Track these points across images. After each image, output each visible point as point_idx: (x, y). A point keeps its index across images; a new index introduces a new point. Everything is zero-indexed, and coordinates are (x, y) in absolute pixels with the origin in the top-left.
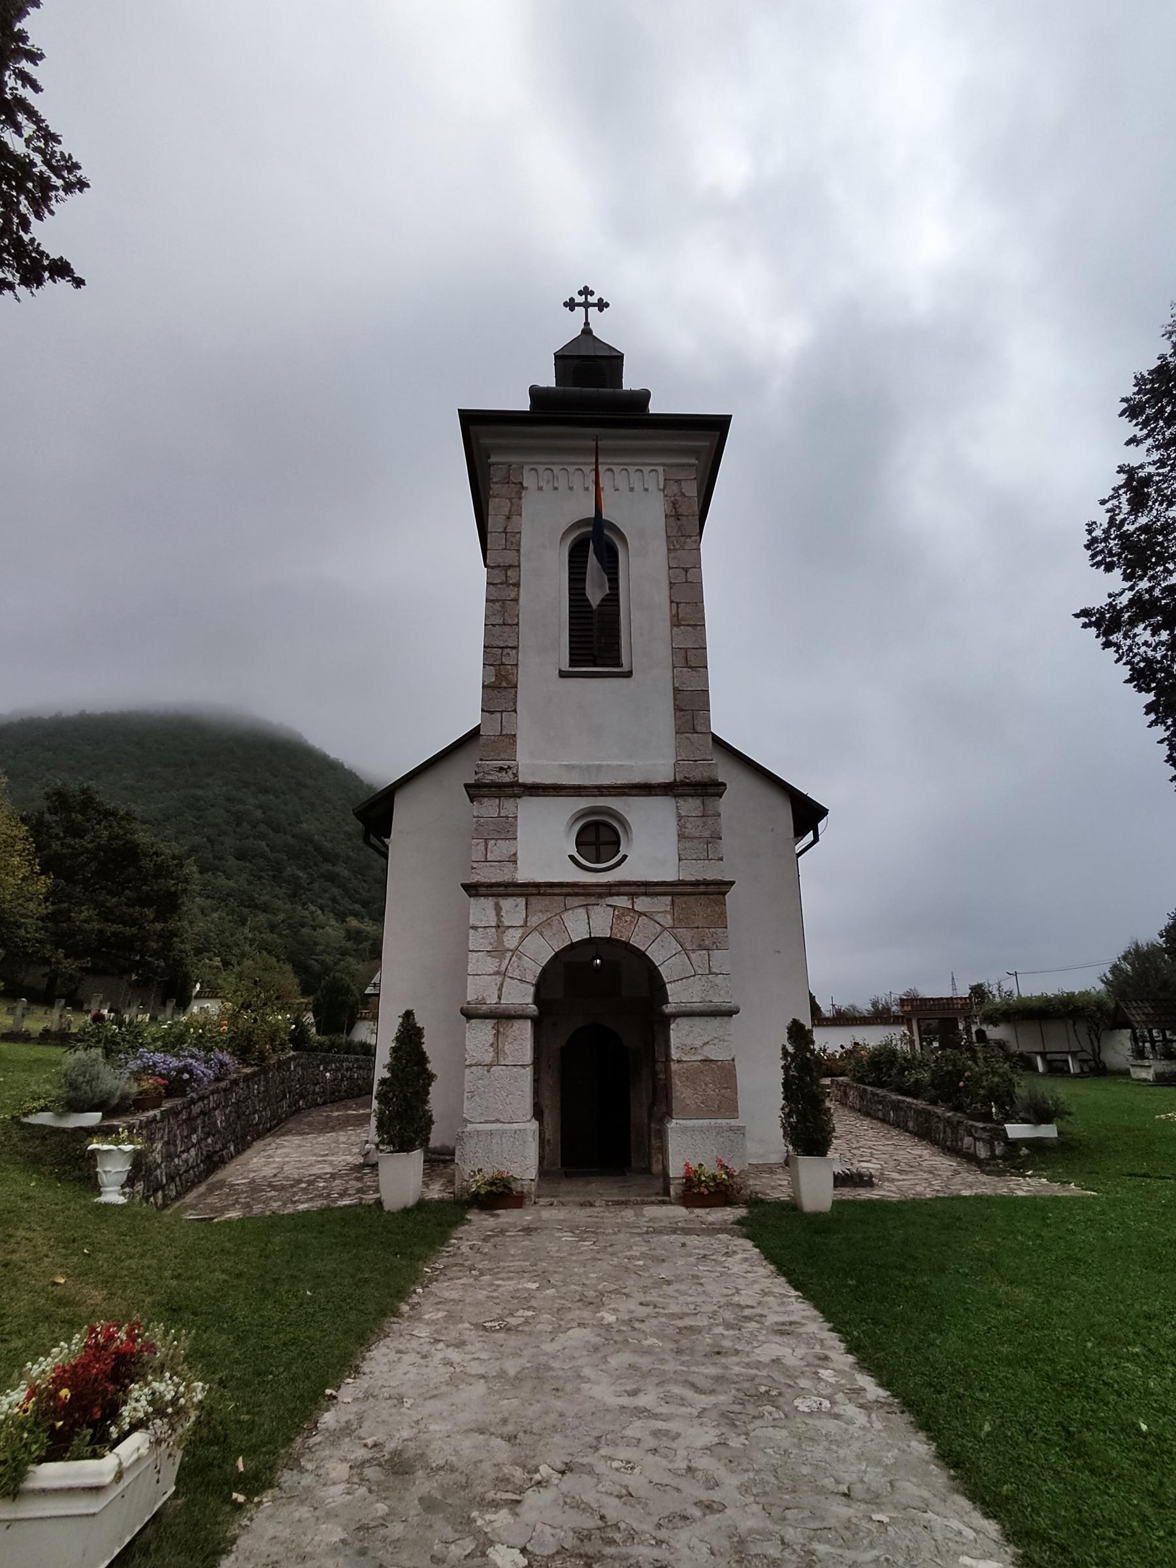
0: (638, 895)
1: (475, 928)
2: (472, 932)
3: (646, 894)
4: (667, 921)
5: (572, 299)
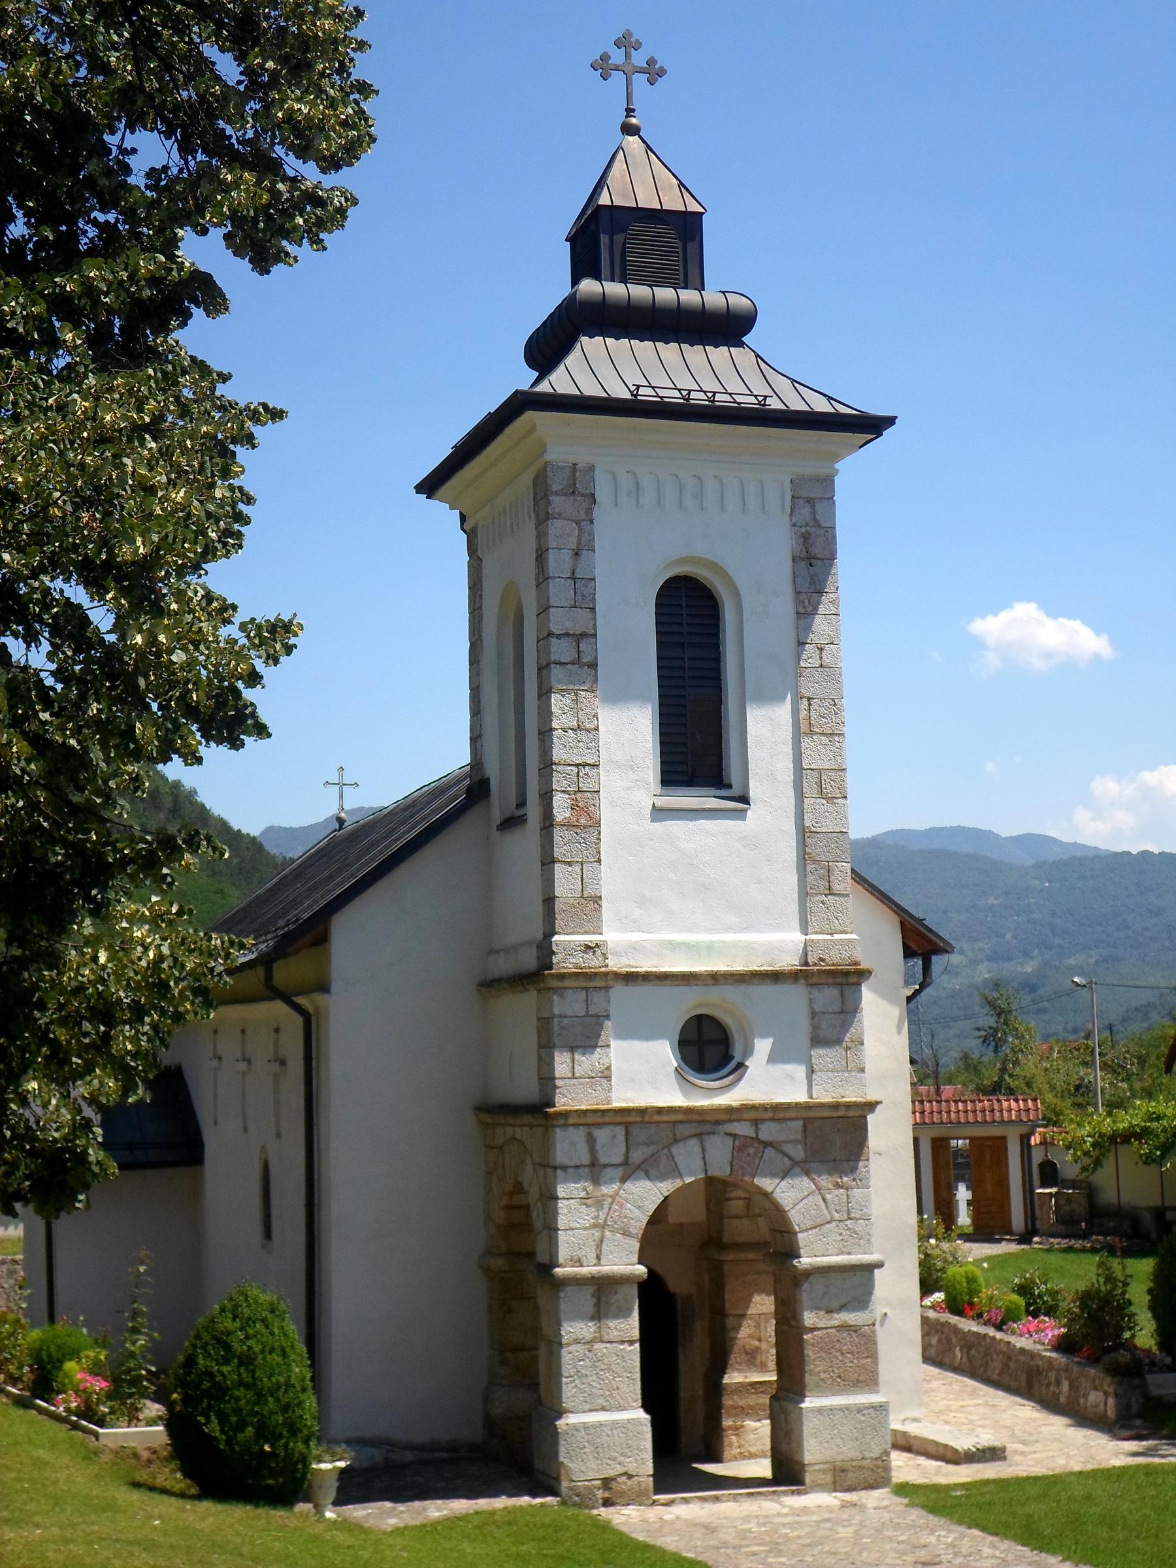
0: (764, 1120)
1: (564, 1168)
2: (559, 1172)
3: (772, 1119)
4: (798, 1152)
5: (605, 57)
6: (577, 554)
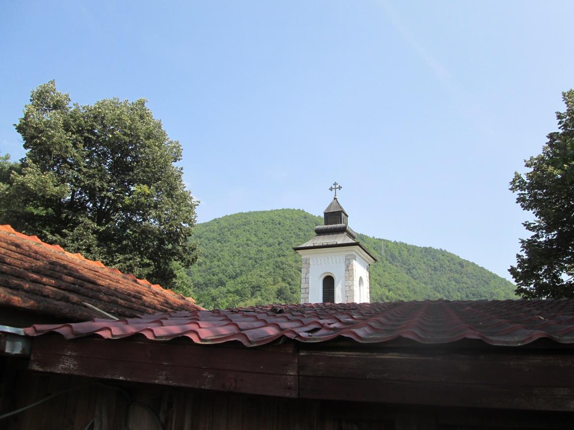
5: (331, 187)
6: (306, 274)
